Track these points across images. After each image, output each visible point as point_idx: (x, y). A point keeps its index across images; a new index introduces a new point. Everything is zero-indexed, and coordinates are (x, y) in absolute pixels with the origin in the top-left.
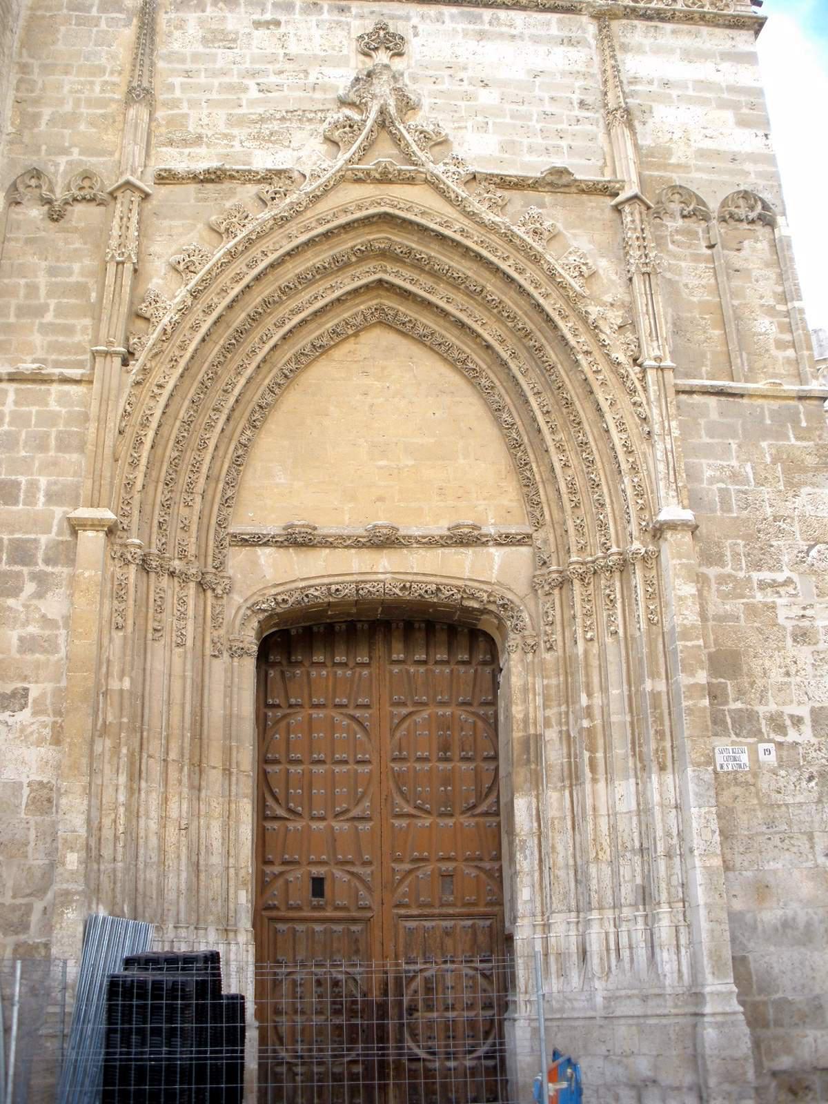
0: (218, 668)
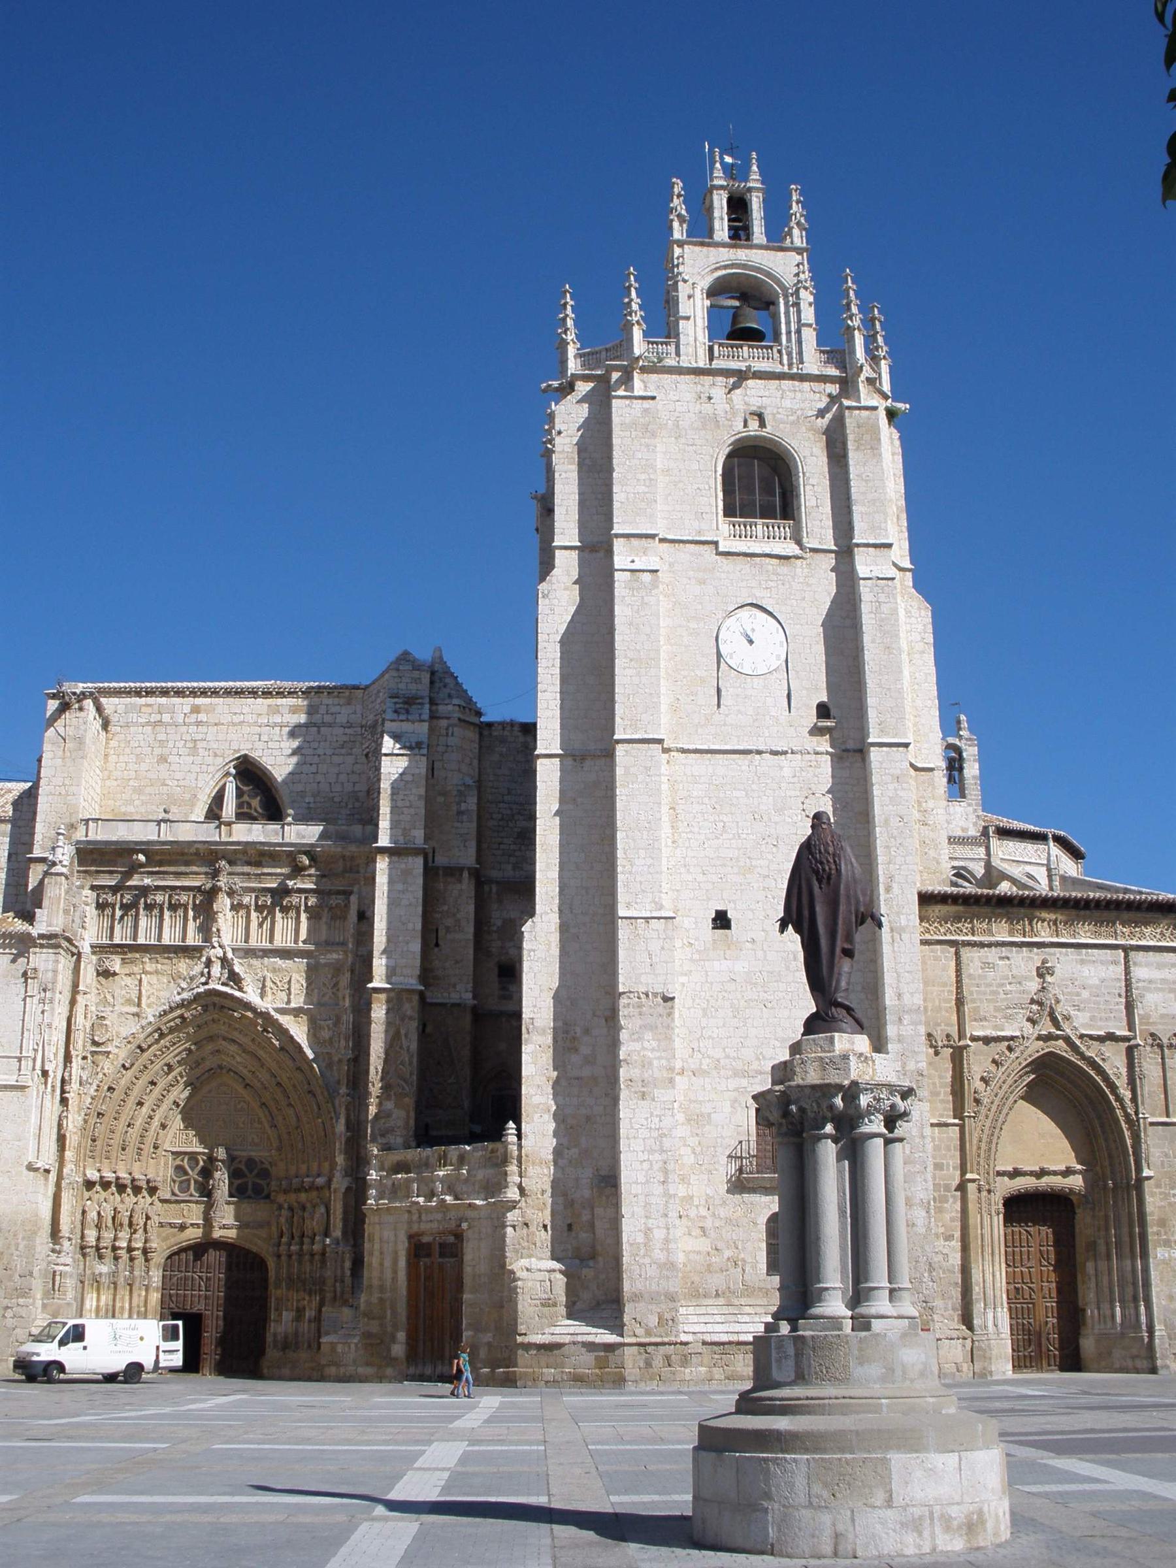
0: (995, 1218)
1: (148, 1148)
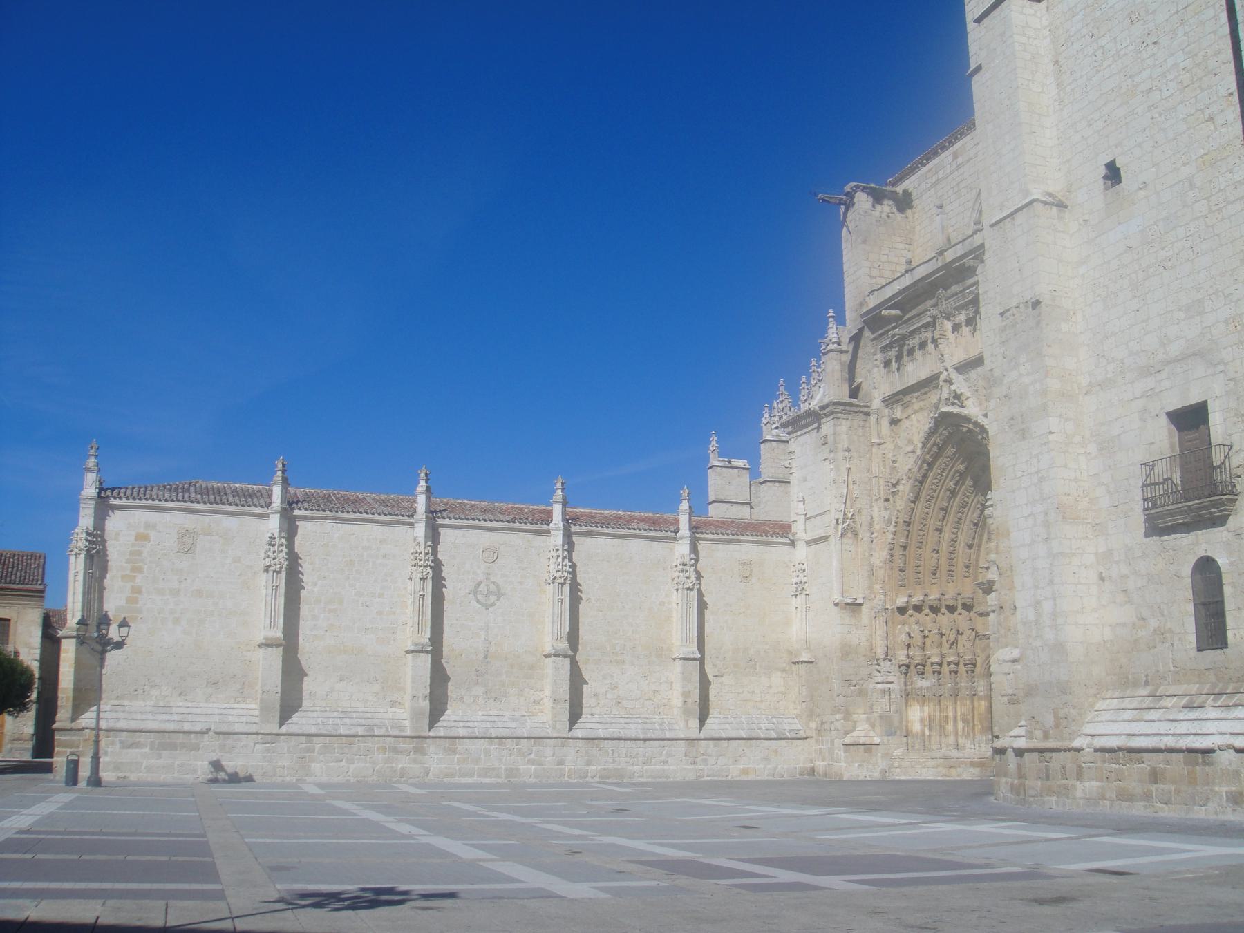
1: (960, 568)
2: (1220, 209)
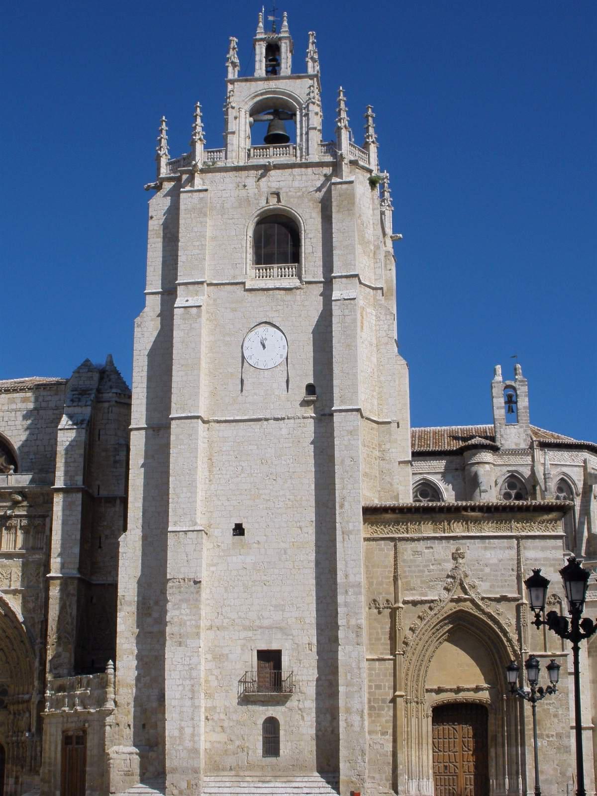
0: (424, 721)
2: (299, 569)
